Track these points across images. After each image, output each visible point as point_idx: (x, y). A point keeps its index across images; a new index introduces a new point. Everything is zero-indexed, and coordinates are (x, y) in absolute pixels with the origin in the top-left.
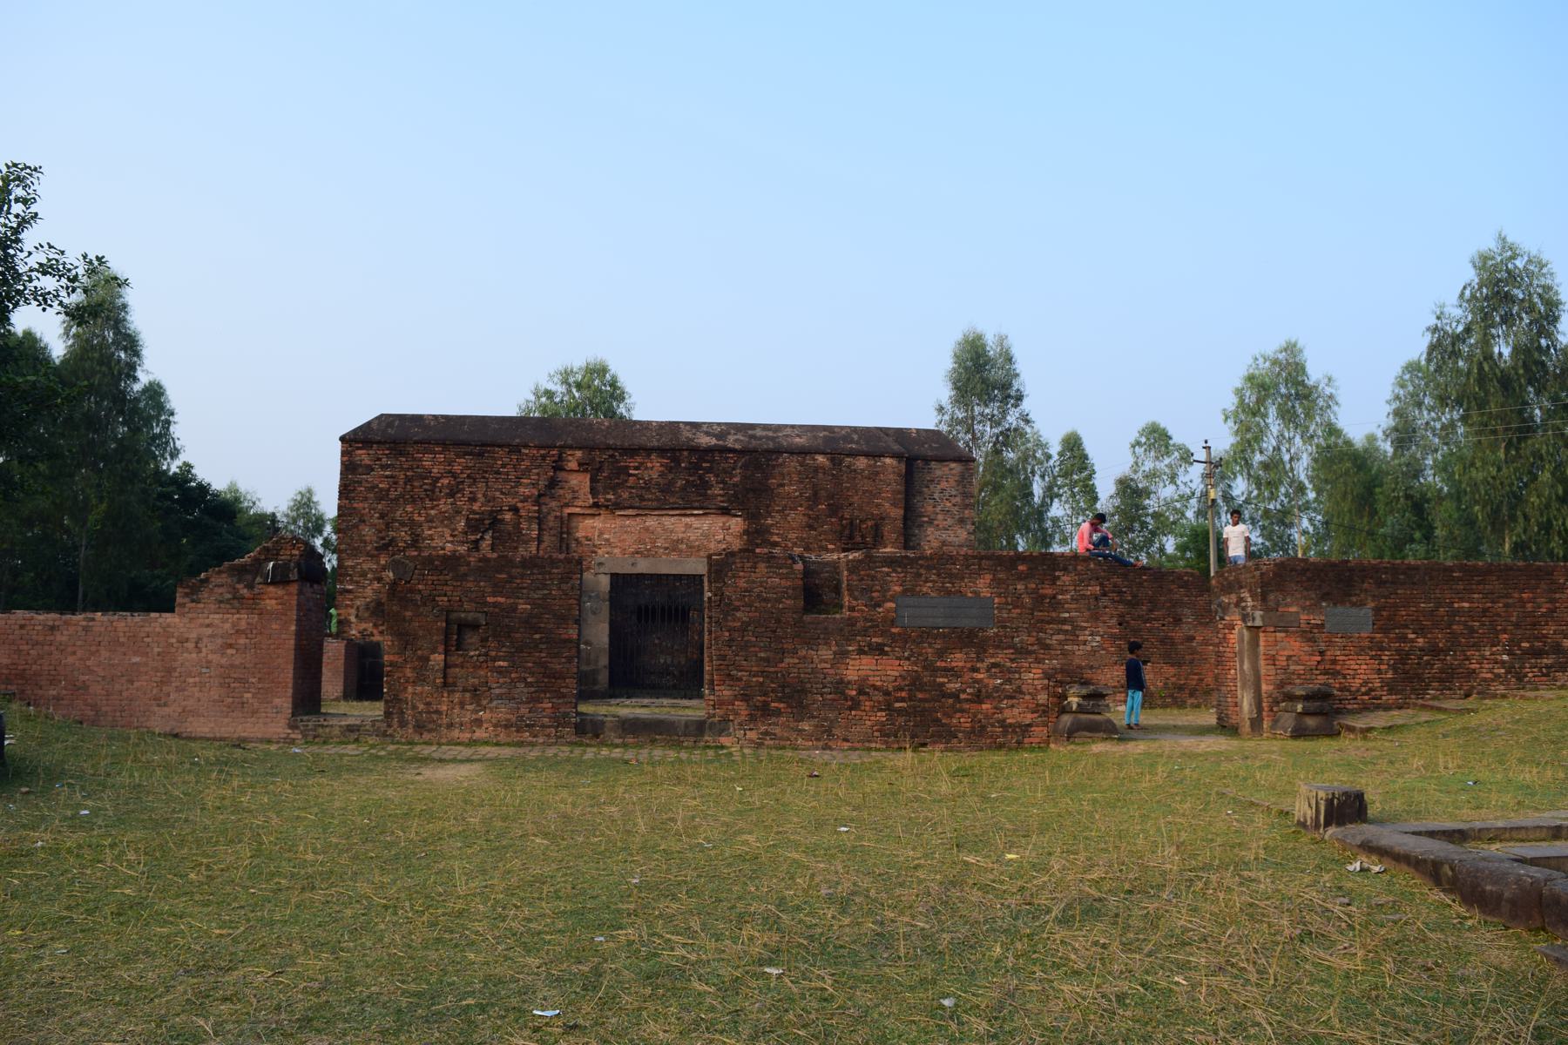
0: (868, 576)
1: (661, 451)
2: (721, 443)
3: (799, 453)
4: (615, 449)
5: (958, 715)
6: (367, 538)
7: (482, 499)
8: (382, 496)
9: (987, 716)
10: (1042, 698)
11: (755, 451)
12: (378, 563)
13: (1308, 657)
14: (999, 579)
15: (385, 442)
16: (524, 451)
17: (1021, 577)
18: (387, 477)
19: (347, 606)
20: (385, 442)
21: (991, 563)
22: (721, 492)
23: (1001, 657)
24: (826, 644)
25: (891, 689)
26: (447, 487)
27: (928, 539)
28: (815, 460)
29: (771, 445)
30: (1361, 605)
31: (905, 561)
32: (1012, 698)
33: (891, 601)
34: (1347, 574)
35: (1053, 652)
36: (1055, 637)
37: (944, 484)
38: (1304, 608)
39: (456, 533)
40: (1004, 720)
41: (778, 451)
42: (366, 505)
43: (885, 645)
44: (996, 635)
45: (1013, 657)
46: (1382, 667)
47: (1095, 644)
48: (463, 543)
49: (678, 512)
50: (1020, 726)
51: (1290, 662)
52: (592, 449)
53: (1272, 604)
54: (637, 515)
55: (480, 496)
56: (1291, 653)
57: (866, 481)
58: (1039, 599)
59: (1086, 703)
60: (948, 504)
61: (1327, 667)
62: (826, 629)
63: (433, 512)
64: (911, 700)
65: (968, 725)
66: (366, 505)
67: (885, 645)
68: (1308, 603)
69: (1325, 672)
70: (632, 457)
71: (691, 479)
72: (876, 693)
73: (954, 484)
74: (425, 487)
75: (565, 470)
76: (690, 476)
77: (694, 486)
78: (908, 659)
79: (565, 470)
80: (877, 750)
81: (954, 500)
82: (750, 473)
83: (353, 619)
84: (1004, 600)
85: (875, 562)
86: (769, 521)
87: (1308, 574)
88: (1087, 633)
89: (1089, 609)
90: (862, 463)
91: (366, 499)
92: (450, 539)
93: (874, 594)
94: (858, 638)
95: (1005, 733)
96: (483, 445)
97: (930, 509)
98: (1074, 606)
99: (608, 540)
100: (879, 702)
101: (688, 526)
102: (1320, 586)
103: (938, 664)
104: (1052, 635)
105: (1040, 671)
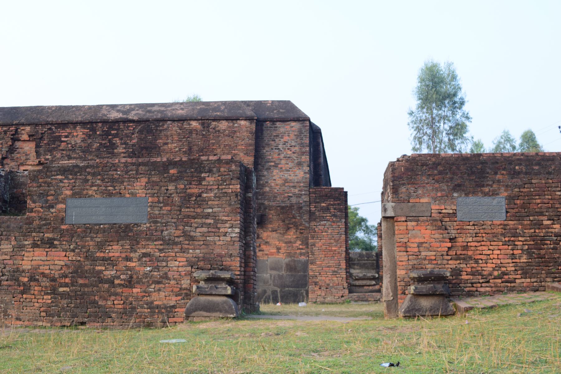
0: (45, 183)
1: (83, 124)
2: (125, 116)
3: (179, 120)
4: (52, 124)
5: (113, 298)
9: (137, 299)
10: (185, 283)
11: (147, 121)
13: (438, 244)
14: (153, 182)
17: (172, 179)
21: (147, 168)
22: (124, 150)
23: (152, 248)
24: (7, 239)
25: (57, 276)
27: (274, 178)
28: (190, 125)
29: (159, 116)
30: (493, 195)
31: (76, 170)
32: (159, 283)
33: (61, 203)
34: (479, 167)
35: (196, 243)
36: (198, 230)
37: (286, 138)
38: (435, 199)
40: (152, 303)
41: (164, 120)
43: (55, 239)
44: (149, 229)
45: (161, 247)
46: (516, 252)
47: (234, 235)
50: (166, 308)
51: (421, 249)
52: (37, 125)
53: (403, 196)
56: (422, 240)
57: (226, 138)
58: (186, 198)
59: (206, 286)
60: (289, 152)
61: (459, 253)
62: (8, 227)
64: (73, 285)
65: (120, 306)
67: (55, 239)
68: (439, 194)
69: (457, 257)
70: (63, 129)
71: (103, 142)
72: (44, 279)
73: (294, 137)
75: (20, 140)
76: (103, 140)
77: (105, 147)
78: (73, 251)
79: (20, 140)
80: (41, 327)
81: (293, 149)
82: (143, 136)
84: (156, 199)
85: (51, 171)
87: (440, 168)
88: (227, 225)
89: (230, 205)
90: (223, 125)
93: (49, 198)
94: (34, 234)
95: (152, 314)
97: (276, 156)
98: (217, 203)
100: (46, 287)
102: (452, 179)
103: (98, 254)
104: (196, 228)
105: (185, 259)
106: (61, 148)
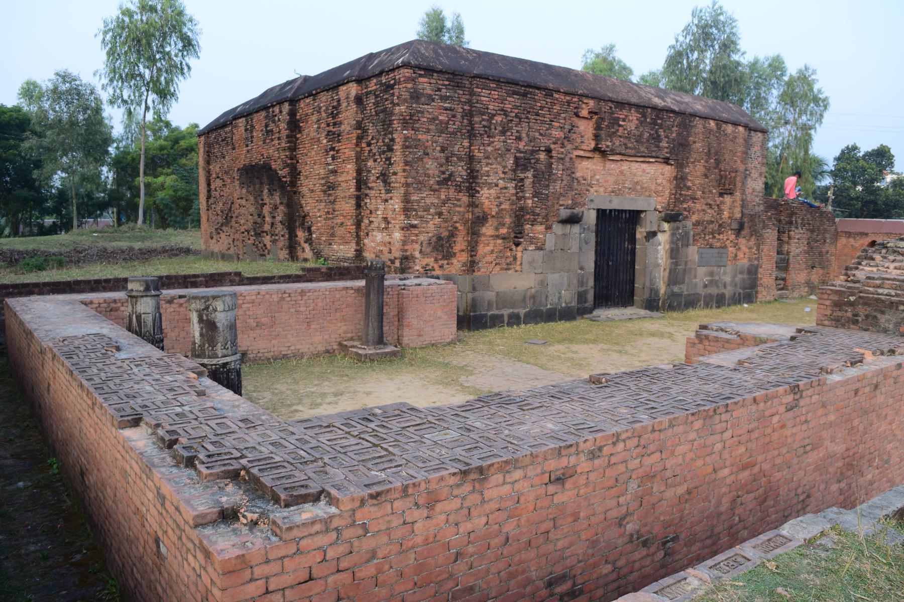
1: (638, 106)
4: (612, 101)
6: (430, 172)
7: (525, 139)
8: (443, 128)
12: (439, 198)
15: (446, 72)
16: (555, 95)
18: (446, 109)
19: (413, 241)
20: (446, 72)
22: (667, 145)
26: (500, 125)
39: (506, 170)
42: (429, 137)
48: (512, 179)
49: (642, 159)
54: (621, 160)
55: (524, 135)
63: (489, 149)
66: (429, 137)
70: (621, 110)
74: (484, 123)
83: (417, 254)
86: (687, 171)
90: (729, 128)
91: (428, 131)
92: (502, 176)
96: (529, 86)
99: (598, 180)
101: (644, 171)
106: (619, 134)
